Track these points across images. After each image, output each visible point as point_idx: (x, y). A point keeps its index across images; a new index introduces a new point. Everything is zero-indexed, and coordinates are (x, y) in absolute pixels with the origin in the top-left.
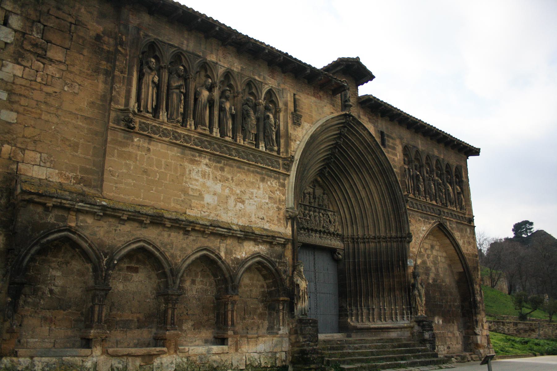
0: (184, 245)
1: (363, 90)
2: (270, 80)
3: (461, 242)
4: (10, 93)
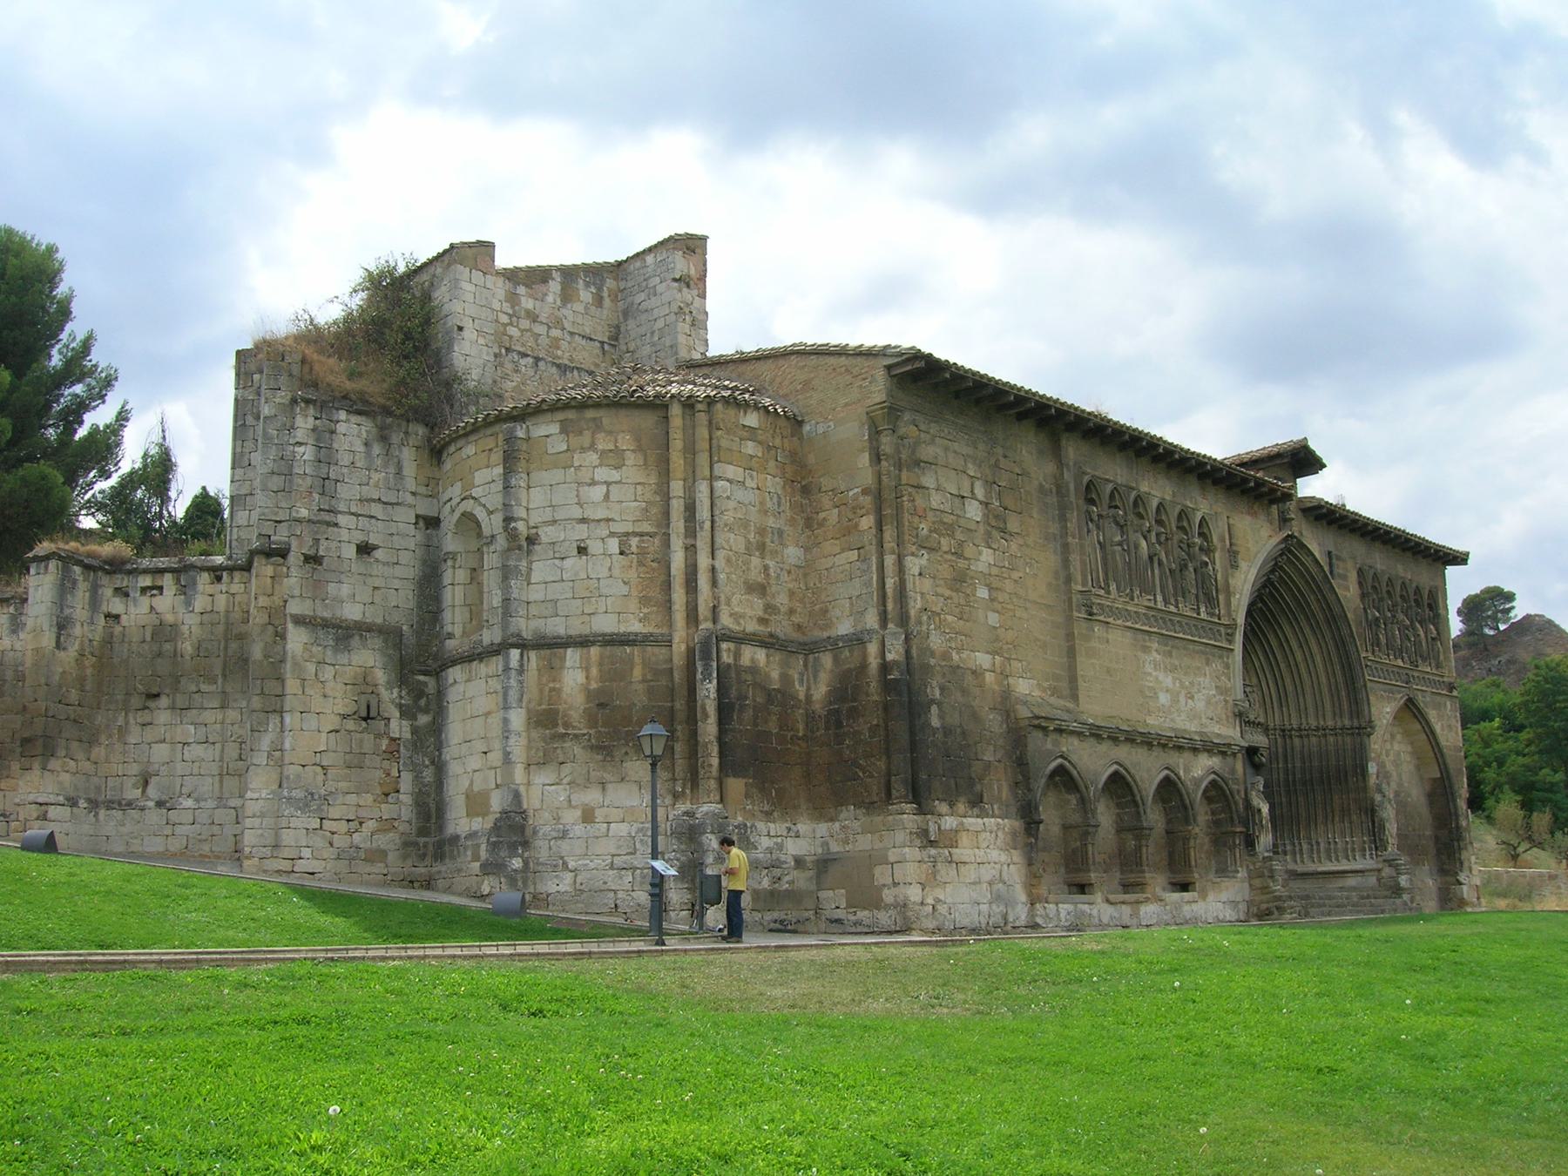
1: (1309, 487)
3: (1438, 728)
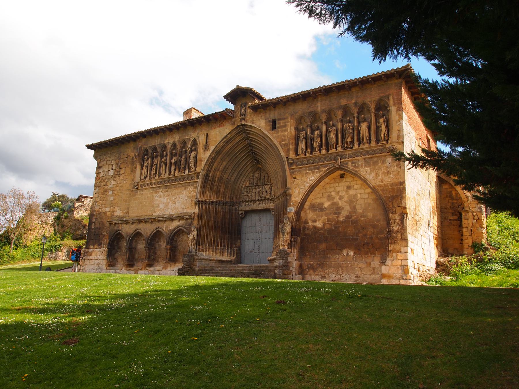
4: (113, 191)
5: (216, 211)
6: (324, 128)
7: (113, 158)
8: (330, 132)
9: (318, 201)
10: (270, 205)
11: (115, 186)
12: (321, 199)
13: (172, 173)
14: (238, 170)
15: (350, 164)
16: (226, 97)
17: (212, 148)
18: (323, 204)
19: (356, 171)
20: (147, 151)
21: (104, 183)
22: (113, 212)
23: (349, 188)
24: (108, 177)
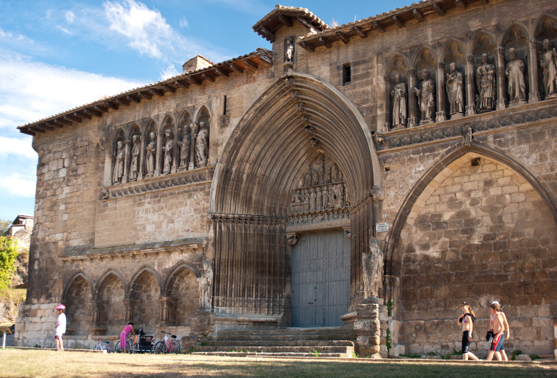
0: (133, 267)
2: (201, 98)
4: (66, 204)
5: (246, 234)
6: (440, 76)
7: (65, 147)
8: (451, 82)
9: (432, 210)
10: (343, 221)
11: (69, 195)
12: (437, 206)
13: (166, 169)
14: (282, 160)
15: (491, 138)
16: (257, 28)
17: (234, 122)
18: (440, 216)
19: (503, 152)
20: (121, 132)
21: (52, 191)
22: (67, 240)
23: (488, 183)
24: (57, 181)
